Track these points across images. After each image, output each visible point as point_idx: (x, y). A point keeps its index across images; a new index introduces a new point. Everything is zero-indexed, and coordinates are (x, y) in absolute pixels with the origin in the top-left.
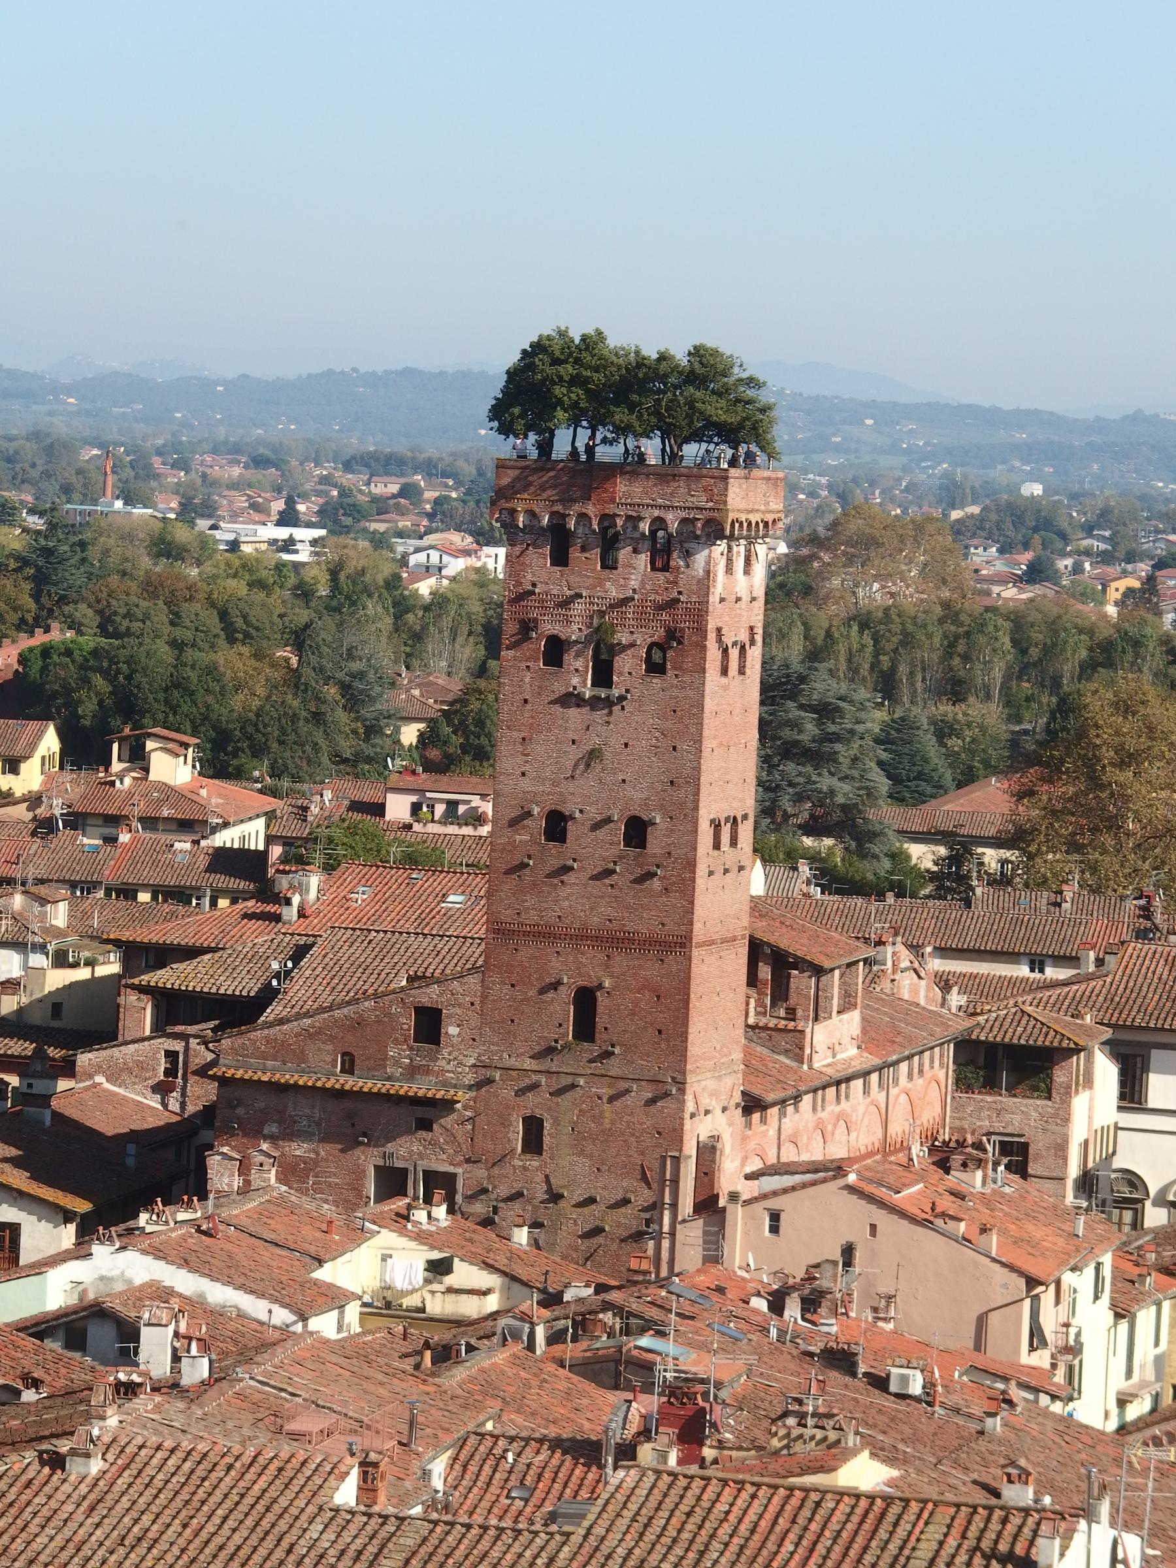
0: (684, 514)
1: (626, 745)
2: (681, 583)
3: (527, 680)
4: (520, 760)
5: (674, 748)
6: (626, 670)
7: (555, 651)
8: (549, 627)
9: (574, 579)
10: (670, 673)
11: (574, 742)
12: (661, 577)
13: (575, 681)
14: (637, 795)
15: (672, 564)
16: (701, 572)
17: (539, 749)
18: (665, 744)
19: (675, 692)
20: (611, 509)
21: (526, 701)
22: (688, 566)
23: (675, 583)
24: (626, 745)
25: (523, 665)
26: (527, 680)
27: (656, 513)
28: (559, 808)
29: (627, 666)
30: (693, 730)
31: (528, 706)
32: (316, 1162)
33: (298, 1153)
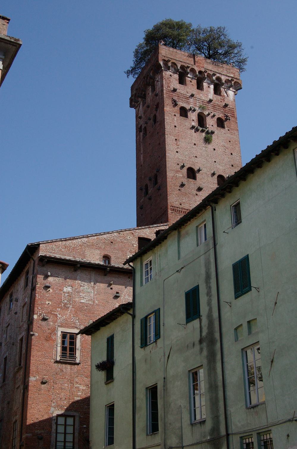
0: (227, 78)
1: (214, 149)
2: (226, 101)
3: (175, 119)
4: (176, 147)
5: (232, 154)
6: (211, 124)
7: (184, 112)
8: (181, 104)
9: (188, 90)
10: (226, 129)
11: (195, 144)
12: (219, 97)
13: (193, 124)
14: (221, 167)
15: (222, 94)
16: (232, 99)
17: (182, 143)
18: (228, 152)
19: (229, 135)
20: (203, 70)
21: (175, 126)
22: (228, 96)
23: (224, 100)
24: (214, 149)
25: (174, 114)
26: (175, 119)
27: (218, 75)
28: (192, 167)
29: (211, 123)
30: (237, 149)
31: (177, 128)
32: (93, 305)
33: (82, 301)
